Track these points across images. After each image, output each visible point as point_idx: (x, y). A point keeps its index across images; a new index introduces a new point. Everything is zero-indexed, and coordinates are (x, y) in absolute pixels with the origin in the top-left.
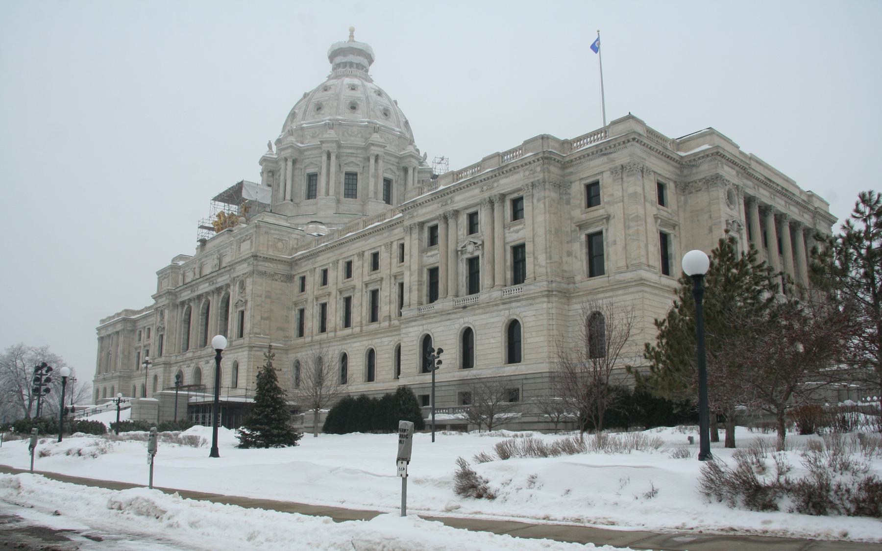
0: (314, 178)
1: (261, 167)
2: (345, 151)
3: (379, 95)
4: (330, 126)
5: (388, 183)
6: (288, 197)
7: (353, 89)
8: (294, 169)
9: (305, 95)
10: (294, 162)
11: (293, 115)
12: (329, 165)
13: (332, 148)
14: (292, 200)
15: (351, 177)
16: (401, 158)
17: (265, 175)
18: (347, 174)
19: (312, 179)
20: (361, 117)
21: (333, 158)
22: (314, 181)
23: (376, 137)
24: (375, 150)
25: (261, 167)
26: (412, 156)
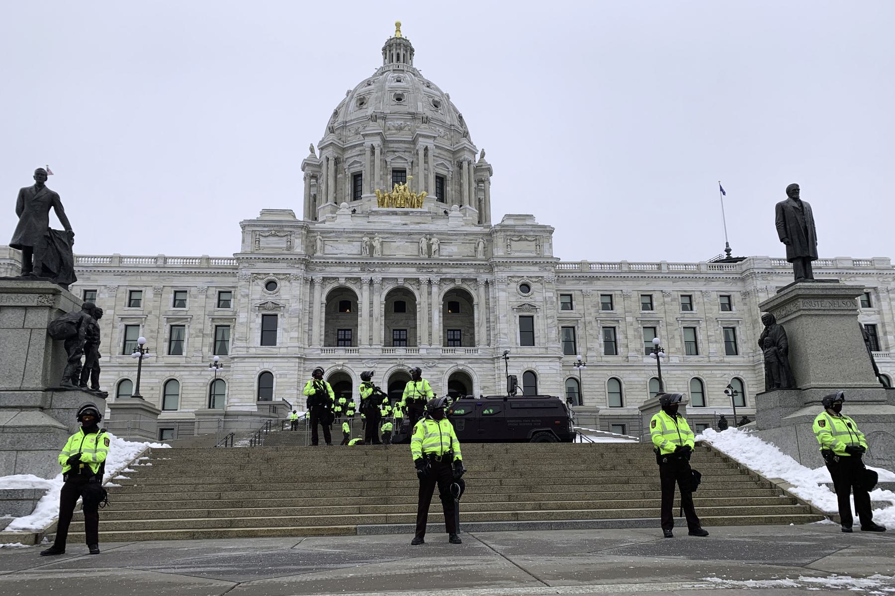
0: (360, 178)
1: (303, 173)
2: (391, 145)
4: (374, 118)
8: (336, 171)
9: (348, 93)
10: (337, 161)
11: (336, 113)
15: (399, 174)
16: (454, 153)
17: (307, 180)
19: (357, 178)
21: (377, 152)
22: (359, 182)
25: (303, 173)
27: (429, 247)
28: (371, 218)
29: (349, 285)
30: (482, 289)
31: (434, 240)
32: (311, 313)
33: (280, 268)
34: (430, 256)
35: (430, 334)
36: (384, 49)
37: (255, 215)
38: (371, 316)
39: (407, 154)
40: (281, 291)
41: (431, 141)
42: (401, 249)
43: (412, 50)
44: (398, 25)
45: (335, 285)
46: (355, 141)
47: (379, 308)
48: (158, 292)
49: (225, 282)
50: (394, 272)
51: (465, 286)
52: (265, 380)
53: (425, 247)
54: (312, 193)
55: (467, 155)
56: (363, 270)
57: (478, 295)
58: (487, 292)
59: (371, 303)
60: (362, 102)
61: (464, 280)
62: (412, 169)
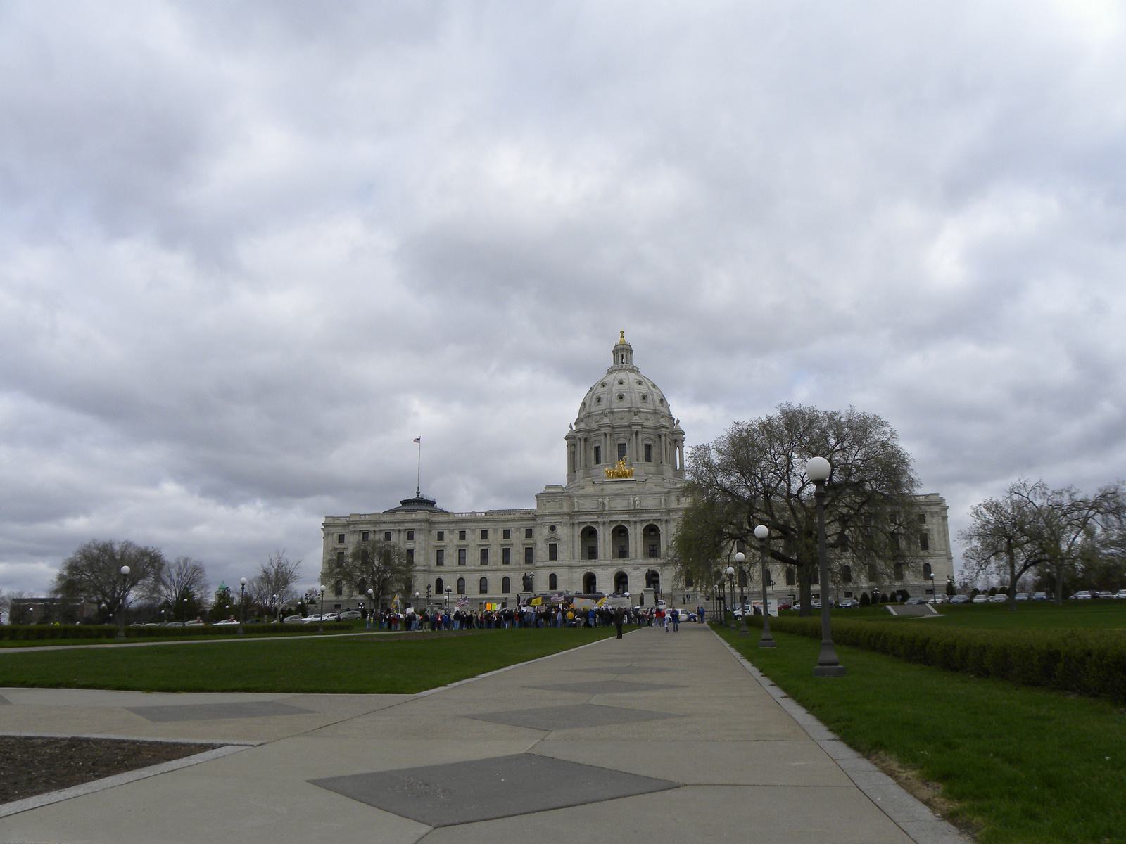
2: (617, 430)
3: (640, 384)
5: (648, 447)
6: (583, 464)
7: (621, 384)
8: (585, 445)
10: (586, 440)
11: (584, 404)
12: (606, 441)
13: (607, 430)
14: (586, 466)
18: (619, 445)
19: (597, 449)
20: (626, 403)
21: (608, 437)
23: (636, 419)
24: (635, 428)
26: (663, 427)
27: (635, 502)
28: (604, 486)
29: (593, 525)
30: (664, 525)
31: (637, 498)
32: (573, 541)
33: (557, 519)
34: (635, 507)
35: (636, 551)
36: (615, 352)
37: (542, 490)
38: (604, 541)
39: (627, 435)
40: (558, 532)
41: (640, 427)
42: (620, 504)
43: (632, 351)
44: (622, 332)
45: (585, 526)
46: (595, 426)
47: (609, 538)
48: (495, 530)
49: (529, 524)
50: (616, 517)
51: (655, 523)
52: (553, 578)
53: (632, 503)
54: (573, 450)
55: (664, 431)
56: (598, 518)
57: (662, 527)
58: (666, 527)
59: (604, 535)
60: (599, 400)
61: (654, 520)
62: (629, 444)
